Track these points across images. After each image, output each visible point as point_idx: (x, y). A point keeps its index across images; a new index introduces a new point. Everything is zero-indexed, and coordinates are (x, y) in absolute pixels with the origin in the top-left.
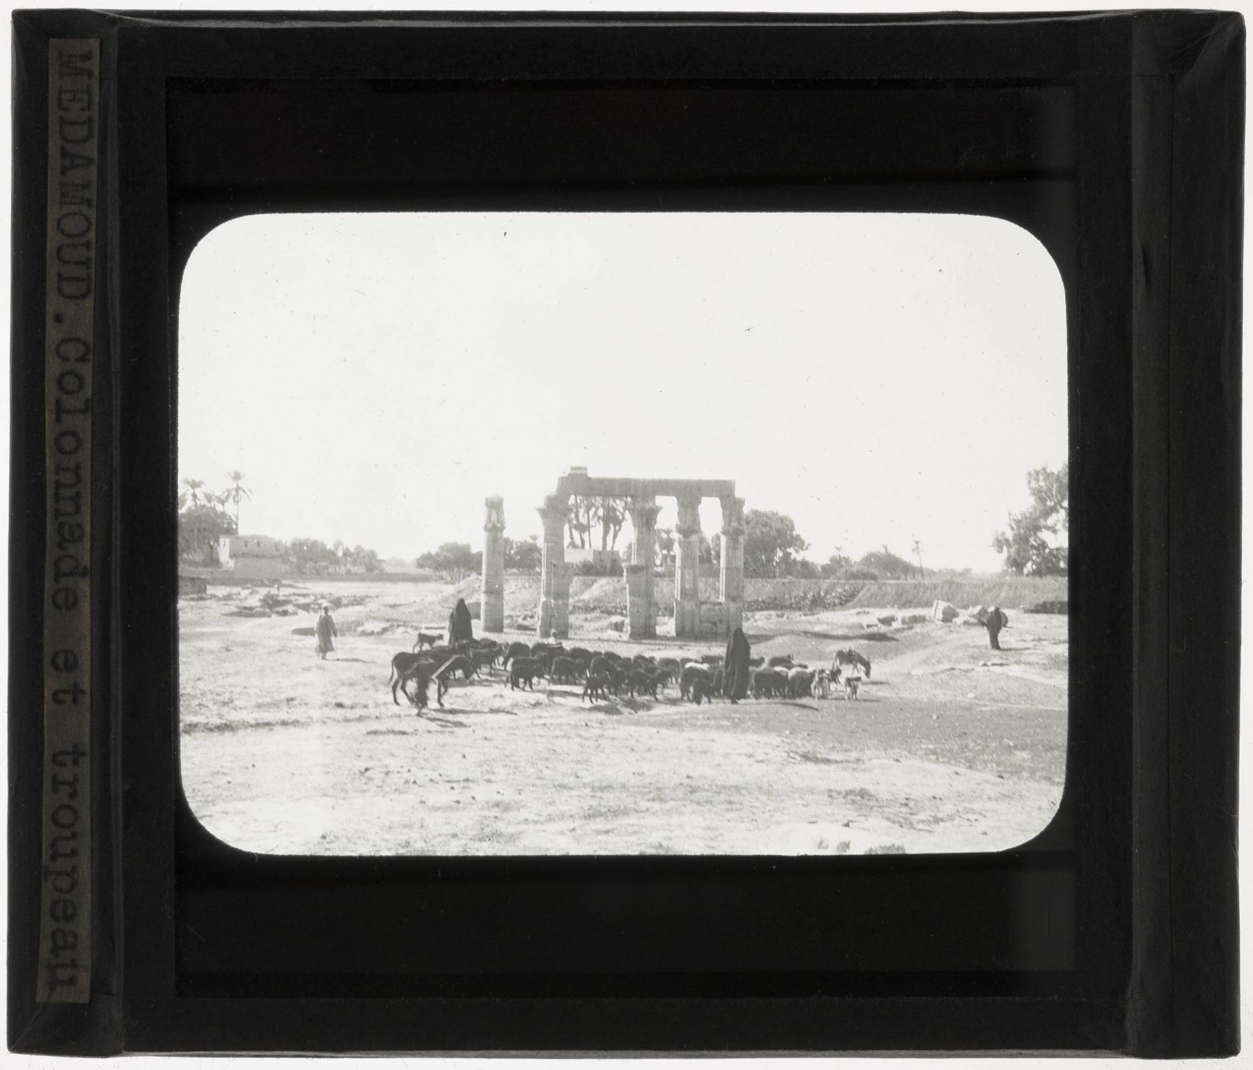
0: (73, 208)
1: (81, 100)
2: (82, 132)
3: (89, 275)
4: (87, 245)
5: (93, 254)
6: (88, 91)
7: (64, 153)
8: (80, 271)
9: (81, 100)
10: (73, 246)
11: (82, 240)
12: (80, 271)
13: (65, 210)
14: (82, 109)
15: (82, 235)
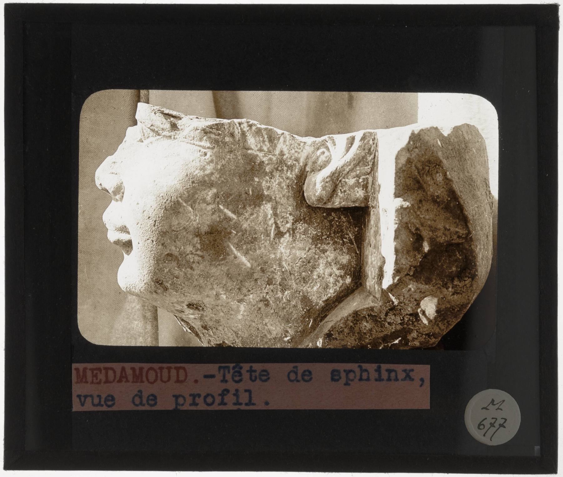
0: (144, 374)
1: (97, 373)
2: (110, 373)
3: (176, 368)
4: (161, 369)
5: (165, 365)
6: (92, 370)
7: (120, 381)
8: (174, 373)
9: (97, 373)
10: (161, 376)
11: (158, 371)
12: (174, 373)
13: (144, 379)
14: (101, 373)
15: (156, 373)
